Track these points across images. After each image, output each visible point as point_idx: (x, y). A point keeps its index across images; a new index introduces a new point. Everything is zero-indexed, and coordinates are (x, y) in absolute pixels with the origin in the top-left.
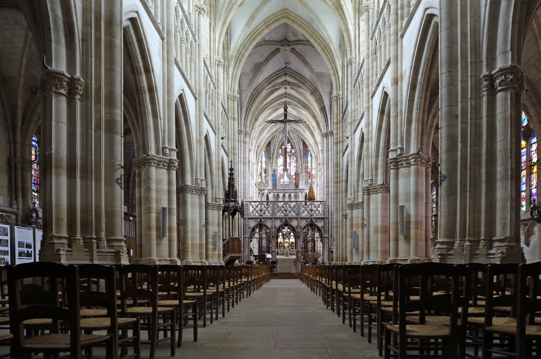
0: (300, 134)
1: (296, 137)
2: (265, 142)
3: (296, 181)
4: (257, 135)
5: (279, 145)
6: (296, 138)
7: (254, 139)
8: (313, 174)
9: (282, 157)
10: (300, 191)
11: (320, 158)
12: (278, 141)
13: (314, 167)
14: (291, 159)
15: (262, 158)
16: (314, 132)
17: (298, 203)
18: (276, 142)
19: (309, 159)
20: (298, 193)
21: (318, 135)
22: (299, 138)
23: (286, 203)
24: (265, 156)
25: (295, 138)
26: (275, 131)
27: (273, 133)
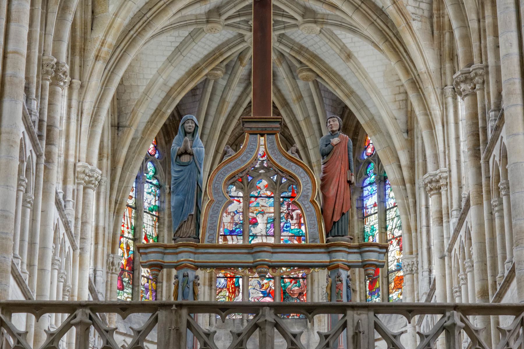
0: (324, 73)
1: (305, 95)
2: (158, 112)
3: (332, 192)
4: (111, 40)
5: (223, 132)
6: (307, 100)
7: (97, 57)
8: (392, 266)
9: (241, 194)
10: (355, 258)
11: (436, 156)
12: (219, 112)
13: (397, 233)
14: (281, 204)
15: (139, 191)
16: (401, 26)
17: (352, 316)
18: (211, 119)
19: (371, 201)
20: (344, 274)
21: (424, 43)
22: (321, 98)
23: (270, 316)
24: (159, 187)
25: (300, 98)
26: (207, 57)
27: (196, 70)
